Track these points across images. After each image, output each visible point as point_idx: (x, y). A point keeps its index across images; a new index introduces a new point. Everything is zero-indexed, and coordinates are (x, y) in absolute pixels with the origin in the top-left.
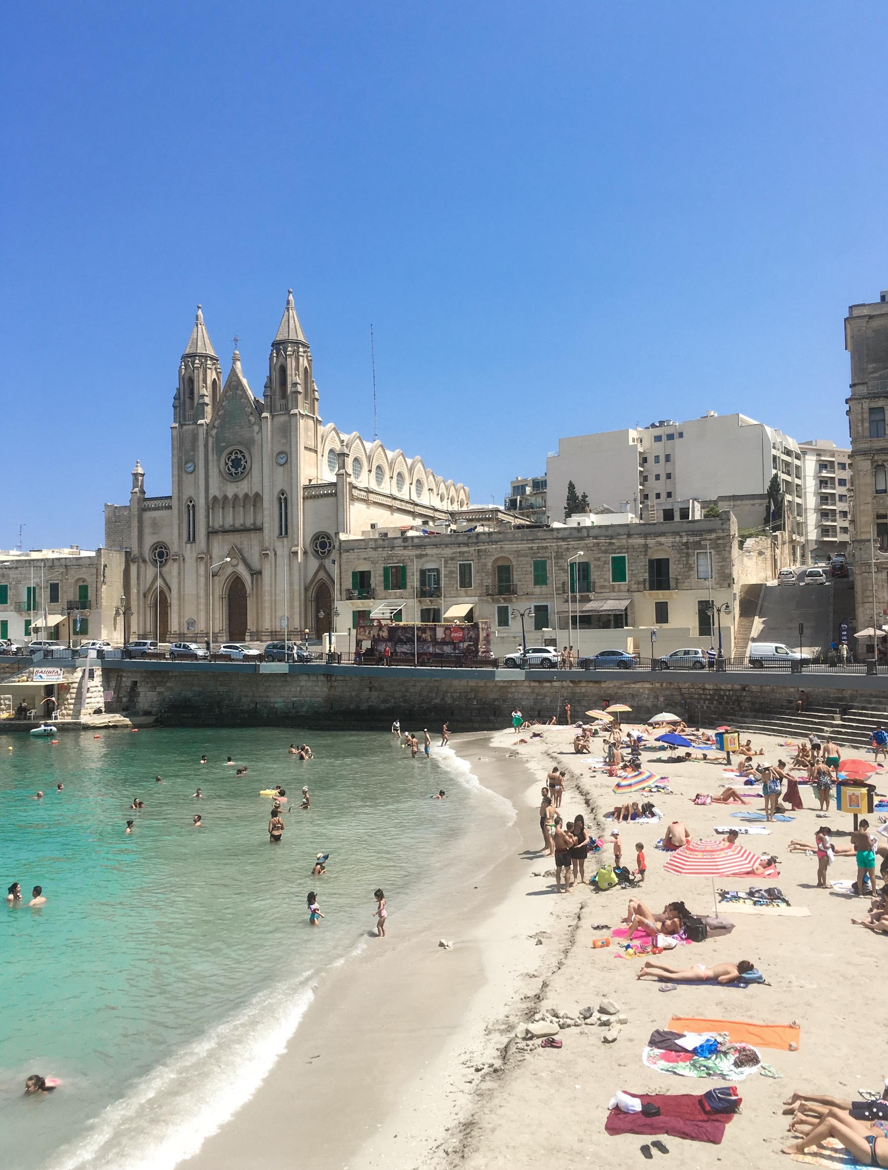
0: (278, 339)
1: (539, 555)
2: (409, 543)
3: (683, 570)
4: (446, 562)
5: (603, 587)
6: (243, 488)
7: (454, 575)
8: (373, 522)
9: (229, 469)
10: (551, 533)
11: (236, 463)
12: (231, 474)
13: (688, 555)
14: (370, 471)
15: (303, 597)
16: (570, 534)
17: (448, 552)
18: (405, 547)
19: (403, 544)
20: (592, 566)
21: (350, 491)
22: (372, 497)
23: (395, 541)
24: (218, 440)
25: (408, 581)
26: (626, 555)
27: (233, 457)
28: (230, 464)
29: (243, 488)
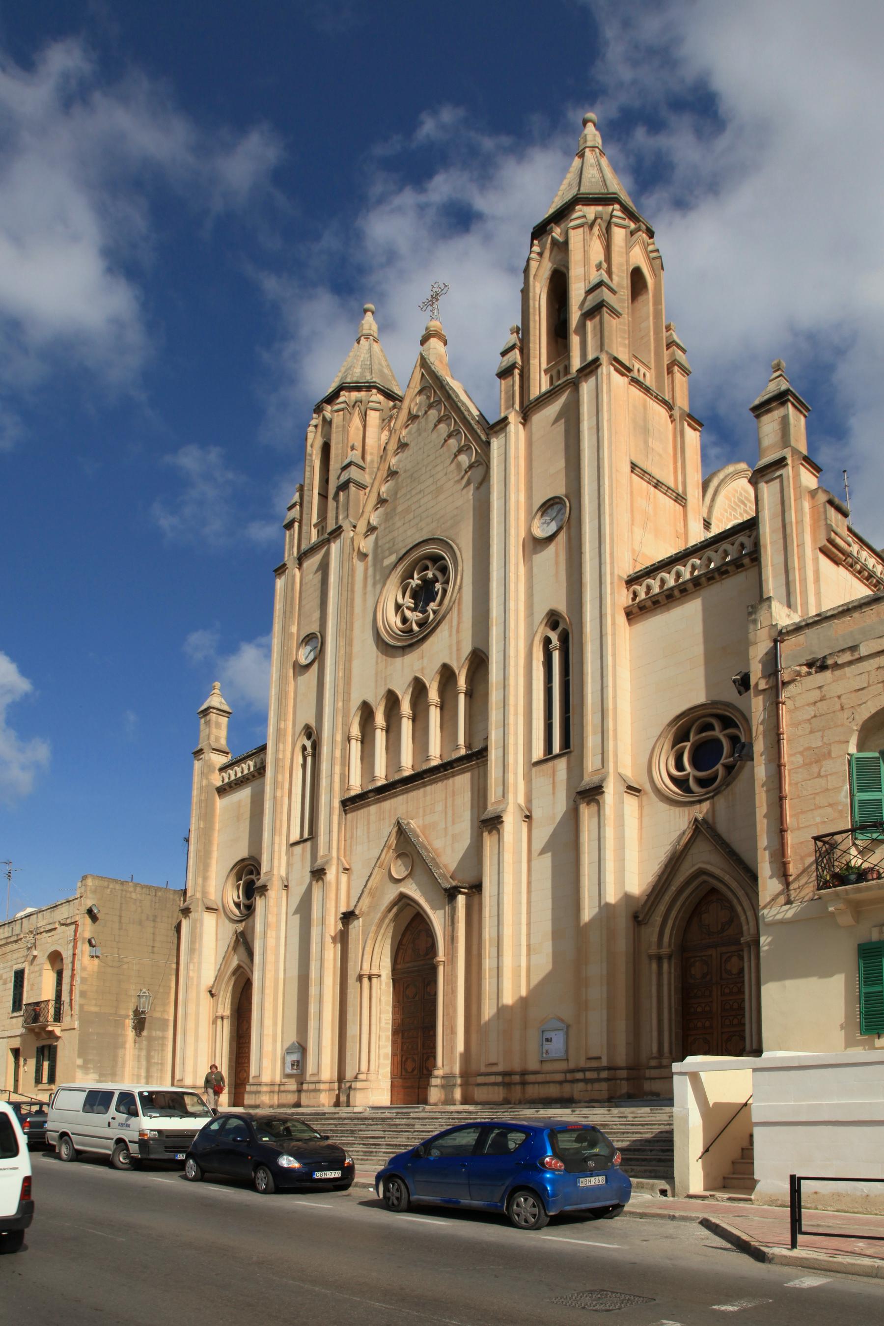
27: (415, 582)
28: (409, 602)
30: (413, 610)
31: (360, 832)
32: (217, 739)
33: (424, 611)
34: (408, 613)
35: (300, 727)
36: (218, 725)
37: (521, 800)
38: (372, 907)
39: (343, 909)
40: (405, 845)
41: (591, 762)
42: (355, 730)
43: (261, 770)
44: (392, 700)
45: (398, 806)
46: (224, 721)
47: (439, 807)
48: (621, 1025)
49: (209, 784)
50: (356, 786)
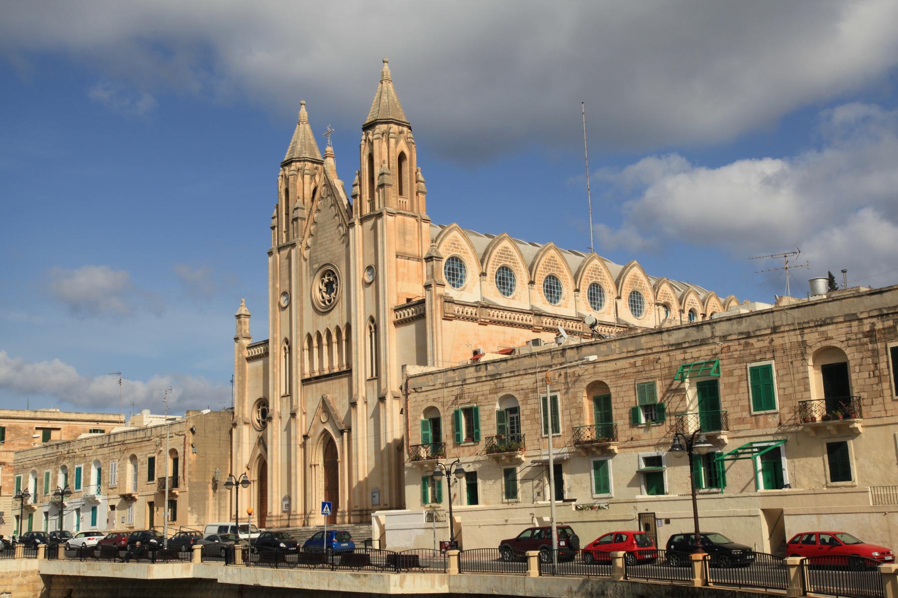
0: (367, 122)
1: (644, 375)
2: (483, 373)
3: (869, 381)
4: (526, 397)
5: (741, 421)
6: (336, 318)
7: (537, 416)
8: (474, 349)
9: (323, 298)
10: (659, 336)
11: (330, 287)
12: (324, 303)
13: (875, 353)
14: (532, 283)
15: (393, 460)
16: (687, 336)
17: (527, 382)
18: (478, 380)
19: (476, 375)
20: (721, 387)
21: (443, 308)
22: (495, 314)
23: (467, 371)
24: (311, 261)
25: (482, 428)
26: (773, 362)
27: (326, 280)
28: (324, 289)
29: (336, 318)
30: (326, 293)
31: (309, 396)
32: (245, 331)
33: (330, 294)
34: (324, 294)
35: (283, 338)
36: (245, 323)
37: (364, 395)
38: (315, 433)
39: (304, 433)
40: (325, 407)
41: (383, 386)
42: (306, 345)
43: (266, 354)
44: (319, 335)
45: (323, 386)
46: (247, 320)
47: (338, 391)
48: (394, 491)
49: (243, 356)
50: (307, 376)
